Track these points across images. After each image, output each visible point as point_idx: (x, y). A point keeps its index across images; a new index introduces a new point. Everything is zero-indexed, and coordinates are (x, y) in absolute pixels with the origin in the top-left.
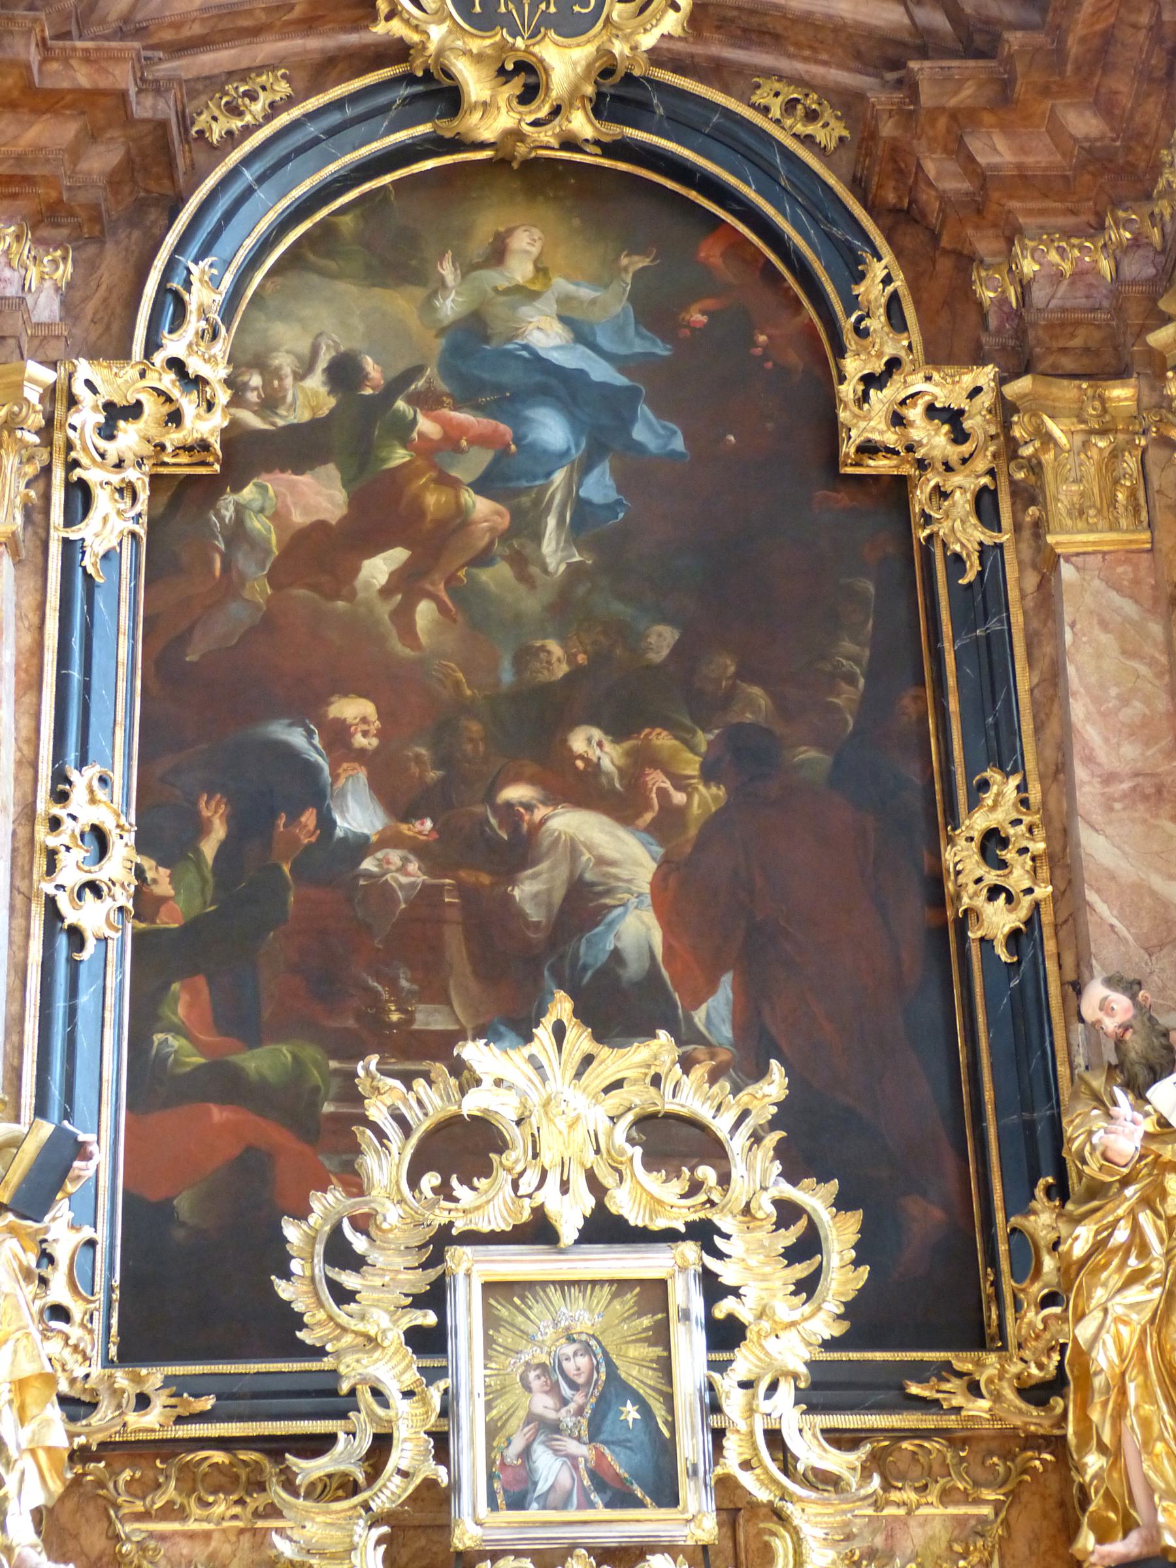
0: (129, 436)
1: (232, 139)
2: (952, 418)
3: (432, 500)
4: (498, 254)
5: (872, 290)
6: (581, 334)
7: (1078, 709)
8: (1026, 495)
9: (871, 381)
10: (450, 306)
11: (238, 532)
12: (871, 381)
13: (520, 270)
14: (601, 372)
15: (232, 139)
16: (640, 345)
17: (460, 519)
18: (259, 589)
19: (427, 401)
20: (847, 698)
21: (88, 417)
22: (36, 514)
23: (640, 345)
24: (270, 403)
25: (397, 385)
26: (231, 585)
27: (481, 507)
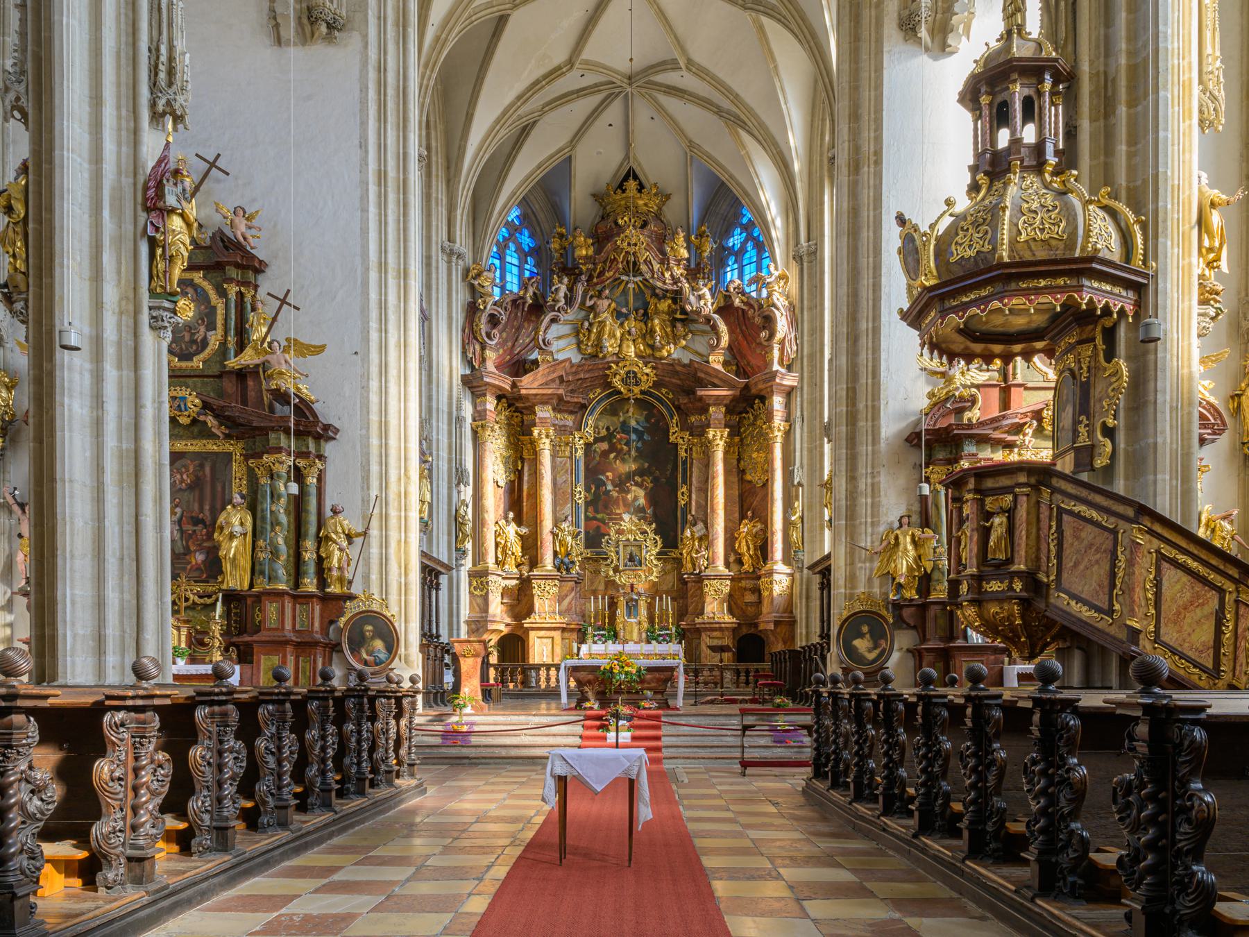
0: (582, 442)
1: (594, 398)
2: (683, 438)
3: (619, 446)
4: (627, 412)
5: (674, 421)
6: (638, 423)
7: (694, 479)
8: (691, 449)
9: (674, 433)
10: (621, 419)
11: (595, 451)
12: (674, 433)
13: (630, 414)
14: (640, 429)
15: (594, 398)
16: (645, 425)
17: (622, 449)
18: (598, 458)
19: (618, 433)
20: (668, 473)
21: (577, 439)
22: (571, 452)
23: (645, 425)
24: (599, 433)
25: (614, 431)
26: (594, 458)
27: (625, 447)
